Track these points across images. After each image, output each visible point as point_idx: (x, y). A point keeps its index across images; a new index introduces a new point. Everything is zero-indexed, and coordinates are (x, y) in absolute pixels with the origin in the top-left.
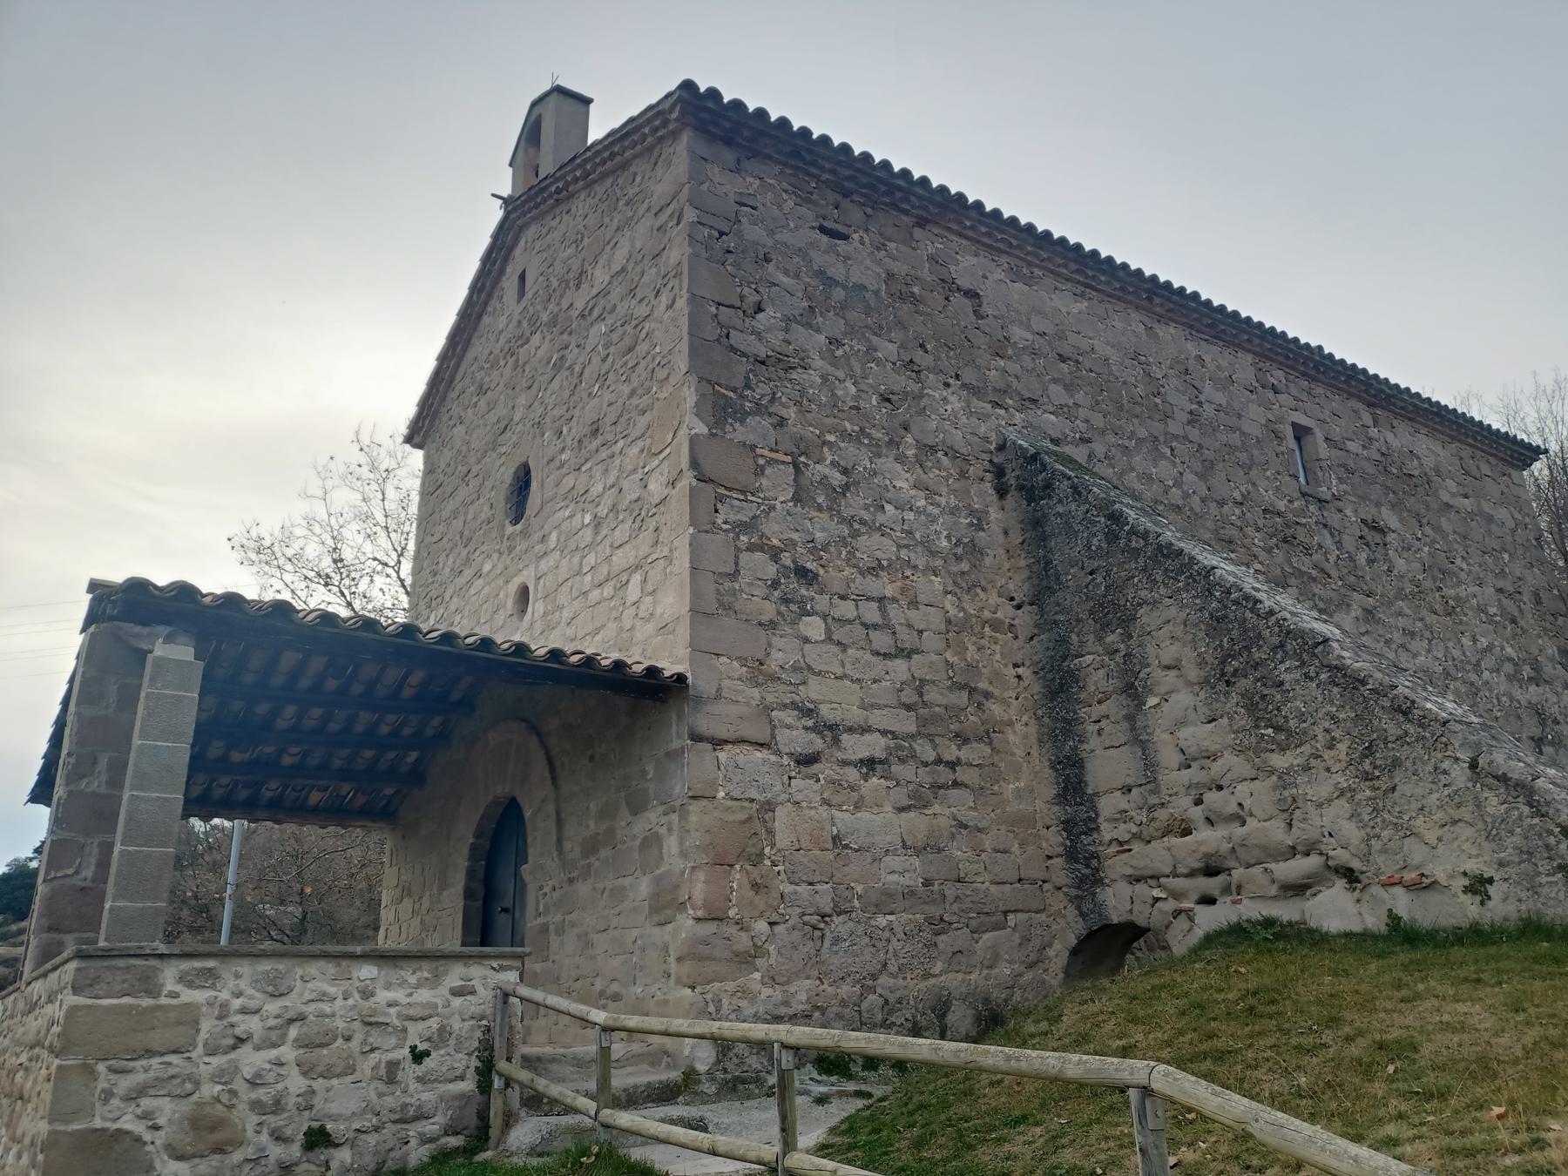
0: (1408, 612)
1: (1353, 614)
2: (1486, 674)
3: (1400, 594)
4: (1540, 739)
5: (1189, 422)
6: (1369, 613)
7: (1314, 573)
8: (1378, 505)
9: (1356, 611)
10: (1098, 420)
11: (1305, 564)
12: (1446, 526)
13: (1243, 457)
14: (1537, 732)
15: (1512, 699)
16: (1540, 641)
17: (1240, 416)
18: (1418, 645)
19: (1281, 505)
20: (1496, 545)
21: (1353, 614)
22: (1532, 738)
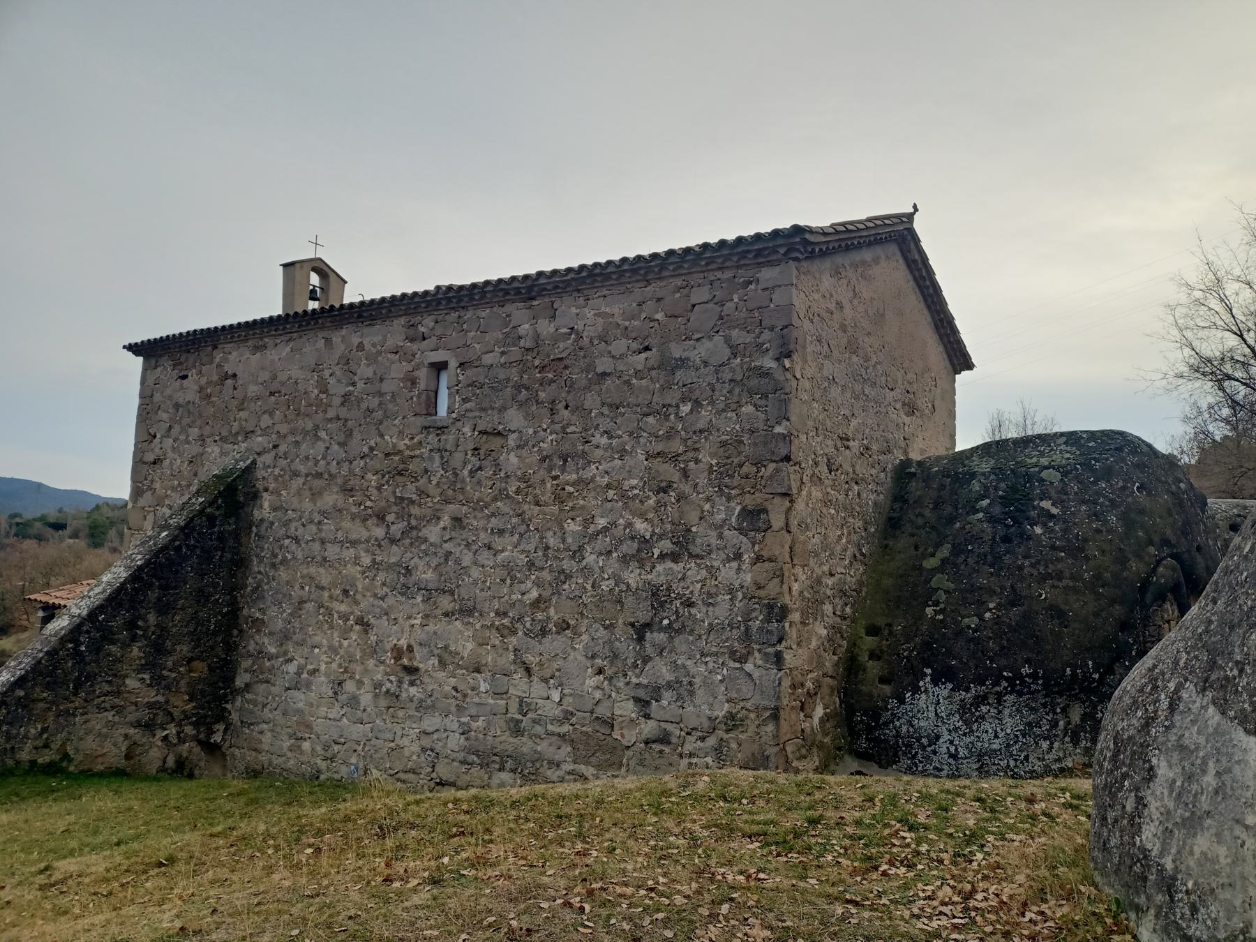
0: (506, 509)
1: (442, 524)
2: (590, 559)
3: (502, 495)
4: (648, 626)
5: (343, 404)
6: (457, 520)
7: (414, 497)
8: (502, 409)
9: (446, 521)
10: (284, 429)
11: (410, 491)
12: (591, 400)
13: (379, 414)
14: (643, 616)
15: (618, 581)
16: (707, 507)
17: (381, 380)
18: (508, 541)
19: (402, 444)
20: (672, 397)
21: (442, 524)
22: (632, 625)
